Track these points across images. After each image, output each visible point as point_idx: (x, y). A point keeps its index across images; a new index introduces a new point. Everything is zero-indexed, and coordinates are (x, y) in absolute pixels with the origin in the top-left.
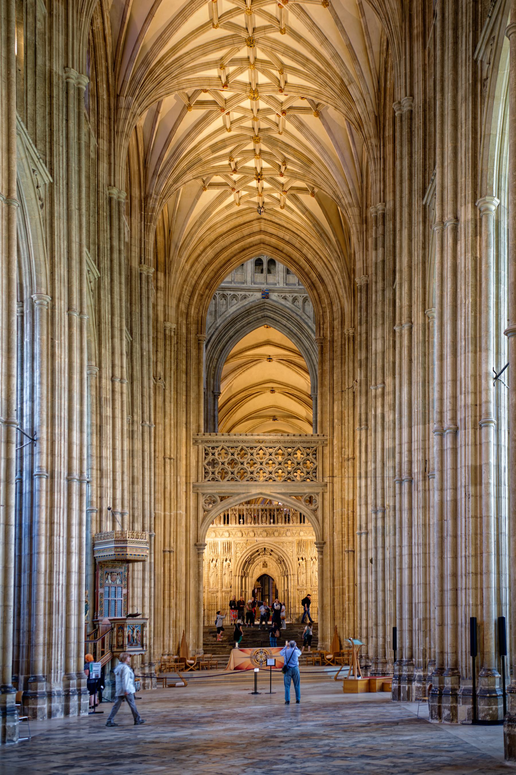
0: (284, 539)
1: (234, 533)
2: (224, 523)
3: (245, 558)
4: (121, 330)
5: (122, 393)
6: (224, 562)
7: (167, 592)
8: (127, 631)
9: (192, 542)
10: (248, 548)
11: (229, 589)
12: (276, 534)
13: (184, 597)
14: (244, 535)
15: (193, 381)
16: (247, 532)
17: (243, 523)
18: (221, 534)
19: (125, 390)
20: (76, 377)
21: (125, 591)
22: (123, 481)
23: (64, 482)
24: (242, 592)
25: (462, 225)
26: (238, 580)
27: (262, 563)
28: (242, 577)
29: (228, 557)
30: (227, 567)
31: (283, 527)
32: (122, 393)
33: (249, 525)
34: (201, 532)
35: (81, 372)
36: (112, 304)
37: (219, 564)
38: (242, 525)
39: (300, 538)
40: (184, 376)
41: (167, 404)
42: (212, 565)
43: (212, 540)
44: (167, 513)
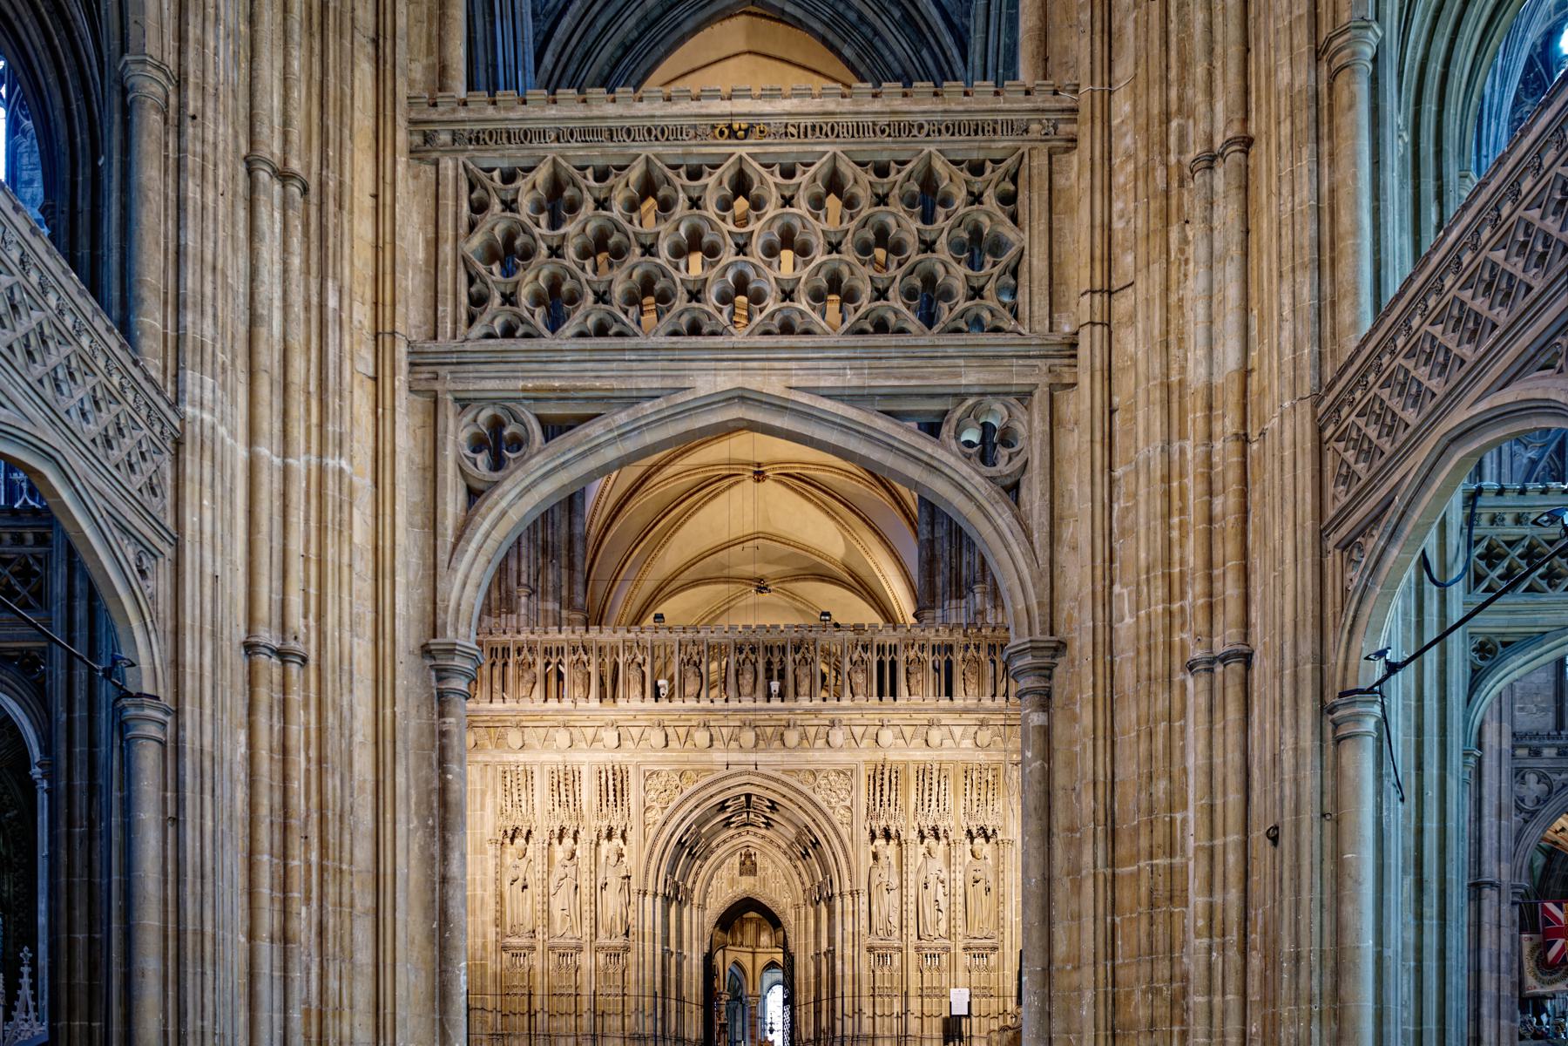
0: (818, 756)
1: (635, 732)
2: (602, 696)
6: (604, 843)
10: (686, 793)
11: (619, 941)
12: (792, 737)
14: (673, 744)
16: (683, 732)
17: (670, 697)
18: (590, 738)
24: (666, 953)
27: (736, 860)
28: (666, 898)
29: (617, 822)
30: (613, 859)
31: (816, 712)
33: (691, 703)
37: (583, 851)
38: (664, 704)
39: (879, 756)
42: (560, 852)
43: (558, 758)
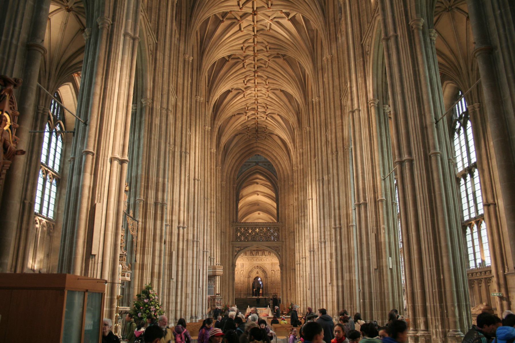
3: (250, 269)
4: (214, 195)
5: (214, 217)
7: (222, 285)
8: (216, 301)
9: (231, 265)
13: (228, 286)
15: (232, 202)
19: (215, 216)
20: (206, 218)
21: (214, 286)
22: (214, 247)
23: (202, 252)
25: (325, 181)
26: (246, 279)
32: (214, 217)
34: (234, 262)
35: (207, 217)
36: (211, 187)
40: (228, 201)
41: (222, 212)
44: (222, 254)
